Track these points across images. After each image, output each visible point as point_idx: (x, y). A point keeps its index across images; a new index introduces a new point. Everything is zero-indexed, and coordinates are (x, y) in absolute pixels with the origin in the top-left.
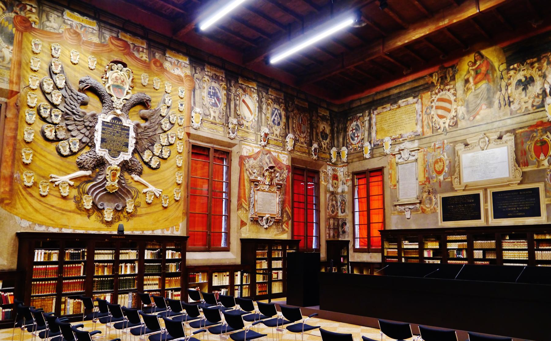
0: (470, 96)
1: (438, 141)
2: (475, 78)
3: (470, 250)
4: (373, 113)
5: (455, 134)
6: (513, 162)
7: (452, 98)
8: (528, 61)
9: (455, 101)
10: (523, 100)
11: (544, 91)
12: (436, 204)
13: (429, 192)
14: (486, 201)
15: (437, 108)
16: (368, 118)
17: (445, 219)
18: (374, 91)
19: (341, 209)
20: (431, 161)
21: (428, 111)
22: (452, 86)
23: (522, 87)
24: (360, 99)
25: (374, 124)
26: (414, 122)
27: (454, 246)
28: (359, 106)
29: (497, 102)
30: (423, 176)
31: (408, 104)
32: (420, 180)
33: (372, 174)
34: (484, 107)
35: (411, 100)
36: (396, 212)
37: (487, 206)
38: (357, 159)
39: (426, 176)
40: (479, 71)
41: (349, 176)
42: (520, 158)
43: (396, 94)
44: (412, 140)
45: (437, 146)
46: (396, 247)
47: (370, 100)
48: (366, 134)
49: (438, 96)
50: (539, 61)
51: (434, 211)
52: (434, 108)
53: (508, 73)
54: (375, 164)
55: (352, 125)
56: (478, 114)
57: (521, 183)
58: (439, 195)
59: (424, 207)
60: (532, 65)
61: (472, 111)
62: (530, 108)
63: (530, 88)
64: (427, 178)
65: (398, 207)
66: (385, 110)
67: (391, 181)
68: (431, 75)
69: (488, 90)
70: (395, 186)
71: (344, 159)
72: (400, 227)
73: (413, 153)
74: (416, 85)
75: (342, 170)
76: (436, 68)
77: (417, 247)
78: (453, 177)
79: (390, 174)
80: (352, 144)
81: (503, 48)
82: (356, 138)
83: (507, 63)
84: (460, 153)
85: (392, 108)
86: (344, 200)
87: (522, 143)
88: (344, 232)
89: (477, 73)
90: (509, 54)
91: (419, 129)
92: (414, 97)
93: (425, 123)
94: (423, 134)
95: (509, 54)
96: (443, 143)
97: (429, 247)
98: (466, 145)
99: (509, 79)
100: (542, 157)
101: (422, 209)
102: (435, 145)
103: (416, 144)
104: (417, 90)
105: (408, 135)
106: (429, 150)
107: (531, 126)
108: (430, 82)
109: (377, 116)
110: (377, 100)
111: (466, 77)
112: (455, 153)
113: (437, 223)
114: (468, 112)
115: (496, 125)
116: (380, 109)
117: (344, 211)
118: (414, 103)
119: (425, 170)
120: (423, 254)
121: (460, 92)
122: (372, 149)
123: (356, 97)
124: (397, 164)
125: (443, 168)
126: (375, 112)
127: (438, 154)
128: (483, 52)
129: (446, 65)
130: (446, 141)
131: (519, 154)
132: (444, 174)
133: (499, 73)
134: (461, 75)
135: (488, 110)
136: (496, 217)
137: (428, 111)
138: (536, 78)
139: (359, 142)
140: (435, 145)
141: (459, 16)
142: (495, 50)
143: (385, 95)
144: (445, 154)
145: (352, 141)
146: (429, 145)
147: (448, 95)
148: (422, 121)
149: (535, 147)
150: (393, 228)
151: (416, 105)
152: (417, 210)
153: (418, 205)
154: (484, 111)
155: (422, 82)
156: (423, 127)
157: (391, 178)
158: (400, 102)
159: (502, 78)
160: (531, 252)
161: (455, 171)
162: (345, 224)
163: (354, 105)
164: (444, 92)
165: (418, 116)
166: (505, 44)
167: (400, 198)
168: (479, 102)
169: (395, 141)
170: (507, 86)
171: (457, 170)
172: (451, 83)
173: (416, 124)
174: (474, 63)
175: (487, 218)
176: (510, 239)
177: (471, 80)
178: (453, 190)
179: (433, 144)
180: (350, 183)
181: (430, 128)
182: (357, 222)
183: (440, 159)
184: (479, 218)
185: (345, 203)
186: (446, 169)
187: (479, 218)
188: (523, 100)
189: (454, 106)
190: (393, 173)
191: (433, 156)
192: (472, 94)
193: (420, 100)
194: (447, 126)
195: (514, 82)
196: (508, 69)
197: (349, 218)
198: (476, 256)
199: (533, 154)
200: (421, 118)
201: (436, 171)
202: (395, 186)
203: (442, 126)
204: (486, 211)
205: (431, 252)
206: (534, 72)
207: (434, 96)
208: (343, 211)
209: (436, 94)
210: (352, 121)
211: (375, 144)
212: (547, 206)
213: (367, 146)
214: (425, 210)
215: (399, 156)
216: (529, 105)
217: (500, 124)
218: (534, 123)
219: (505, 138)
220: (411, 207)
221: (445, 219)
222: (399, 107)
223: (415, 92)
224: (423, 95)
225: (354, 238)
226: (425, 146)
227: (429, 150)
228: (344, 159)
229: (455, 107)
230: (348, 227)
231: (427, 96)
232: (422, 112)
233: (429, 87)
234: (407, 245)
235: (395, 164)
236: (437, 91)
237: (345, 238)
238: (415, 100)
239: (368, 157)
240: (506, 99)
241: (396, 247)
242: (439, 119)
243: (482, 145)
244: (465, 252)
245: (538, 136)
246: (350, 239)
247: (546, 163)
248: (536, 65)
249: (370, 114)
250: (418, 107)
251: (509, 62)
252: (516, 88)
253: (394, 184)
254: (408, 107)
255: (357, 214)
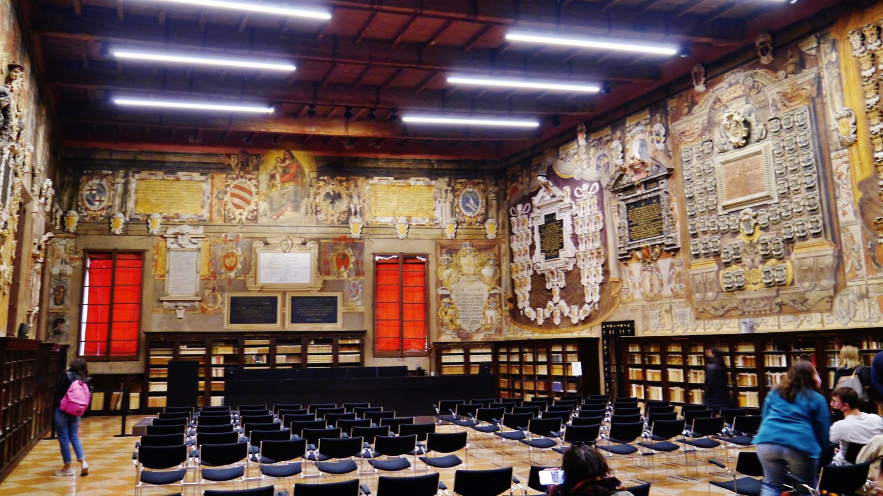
0: (275, 193)
1: (230, 232)
2: (282, 176)
3: (271, 356)
4: (133, 176)
5: (253, 229)
6: (315, 269)
7: (254, 190)
8: (338, 178)
9: (257, 193)
10: (331, 212)
11: (350, 210)
12: (223, 303)
13: (214, 289)
14: (284, 305)
15: (233, 195)
16: (123, 181)
17: (233, 321)
18: (136, 148)
19: (55, 299)
20: (219, 253)
21: (221, 196)
22: (254, 177)
23: (330, 201)
24: (111, 151)
25: (133, 191)
26: (199, 204)
27: (254, 351)
28: (106, 160)
29: (303, 208)
30: (206, 269)
31: (191, 180)
32: (201, 273)
33: (121, 256)
34: (290, 209)
35: (196, 176)
36: (161, 309)
37: (284, 310)
38: (95, 232)
39: (212, 270)
40: (287, 170)
41: (76, 253)
42: (322, 267)
43: (175, 162)
44: (195, 225)
45: (229, 238)
46: (170, 353)
47: (130, 157)
48: (118, 201)
49: (236, 182)
50: (347, 180)
51: (219, 313)
52: (229, 194)
53: (317, 183)
54: (132, 243)
55: (91, 182)
56: (282, 214)
57: (321, 290)
58: (227, 294)
59: (205, 306)
60: (341, 182)
61: (276, 210)
62: (335, 221)
63: (337, 203)
64: (212, 273)
65: (165, 304)
66: (154, 178)
67: (156, 269)
68: (229, 156)
69: (296, 193)
70: (163, 276)
71: (72, 227)
72: (165, 329)
73: (194, 241)
74: (206, 160)
75: (63, 242)
76: (237, 151)
77: (203, 352)
78: (248, 276)
79: (156, 261)
80: (87, 209)
81: (315, 157)
82: (97, 203)
83: (318, 172)
84: (258, 251)
85: (166, 177)
86: (63, 287)
87: (326, 253)
88: (58, 333)
89: (285, 173)
90: (321, 164)
91: (205, 213)
92: (202, 174)
93: (215, 208)
94: (211, 220)
95: (321, 164)
96: (238, 237)
97: (219, 353)
98: (266, 244)
99: (318, 189)
100: (342, 269)
101: (202, 308)
102: (226, 236)
103: (200, 231)
104: (207, 166)
105: (188, 216)
106: (217, 241)
107: (335, 239)
108: (226, 163)
109: (140, 182)
110: (141, 161)
111: (272, 172)
112: (251, 250)
113: (222, 324)
114: (271, 209)
115: (301, 230)
116: (145, 174)
117: (62, 303)
118: (201, 181)
119: (212, 262)
120: (210, 360)
121: (263, 186)
122: (126, 224)
123: (105, 145)
124: (169, 250)
125: (235, 266)
126: (137, 176)
127: (230, 247)
128: (294, 153)
129: (249, 151)
130: (241, 235)
131: (322, 263)
132: (236, 271)
133: (308, 180)
134: (266, 168)
135: (293, 214)
136: (293, 322)
137: (221, 196)
138: (344, 195)
139: (103, 209)
140: (226, 236)
141: (327, 130)
142: (307, 156)
143: (157, 158)
144: (239, 249)
145: (88, 205)
146: (218, 235)
147: (250, 185)
148: (211, 205)
149: (337, 259)
150: (155, 329)
151: (204, 185)
152: (194, 309)
153: (197, 304)
154: (289, 214)
155: (214, 160)
156: (211, 212)
157: (156, 265)
158: (180, 174)
159: (311, 186)
160: (335, 354)
161: (250, 270)
162: (63, 321)
163: (98, 156)
164: (244, 180)
165: (205, 198)
166: (319, 154)
167: (169, 292)
168: (284, 202)
169: (167, 221)
170: (316, 194)
171: (253, 268)
172: (254, 172)
173: (202, 207)
174: (284, 161)
175: (284, 323)
176: (315, 343)
177: (278, 177)
178: (245, 289)
179: (223, 235)
180: (78, 263)
181: (220, 215)
182: (85, 319)
183: (233, 254)
184: (274, 321)
185: (65, 291)
186: (239, 266)
187: (274, 321)
188: (331, 212)
189: (255, 199)
190: (160, 260)
191: (223, 248)
192: (277, 192)
193: (210, 180)
194: (244, 219)
195: (323, 194)
196: (318, 180)
197: (74, 311)
198: (278, 362)
199: (335, 264)
200: (209, 201)
201: (226, 267)
202: (163, 276)
203: (238, 217)
204: (284, 315)
205: (222, 359)
206: (341, 190)
207: (230, 181)
208: (59, 302)
209: (233, 179)
210: (91, 177)
211: (134, 216)
212: (344, 314)
213: (120, 220)
214: (206, 309)
215: (173, 240)
216: (335, 219)
217: (305, 230)
218: (338, 236)
219: (309, 244)
220: (187, 305)
221: (233, 321)
222: (178, 179)
223: (205, 168)
224: (215, 176)
225: (79, 341)
226: (212, 234)
227: (217, 241)
228: (72, 227)
229: (256, 200)
230: (68, 326)
231: (220, 178)
232: (212, 194)
233: (224, 168)
234: (185, 351)
235: (164, 250)
236: (234, 176)
237: (59, 341)
238: (203, 178)
239: (118, 232)
240: (314, 207)
241: (170, 353)
242: (234, 209)
243: (284, 247)
244: (265, 358)
245: (340, 249)
246: (72, 343)
247: (345, 275)
248: (345, 184)
249: (126, 176)
250: (206, 187)
251: (321, 172)
252: (325, 200)
253: (161, 273)
254: (191, 184)
255: (85, 309)
